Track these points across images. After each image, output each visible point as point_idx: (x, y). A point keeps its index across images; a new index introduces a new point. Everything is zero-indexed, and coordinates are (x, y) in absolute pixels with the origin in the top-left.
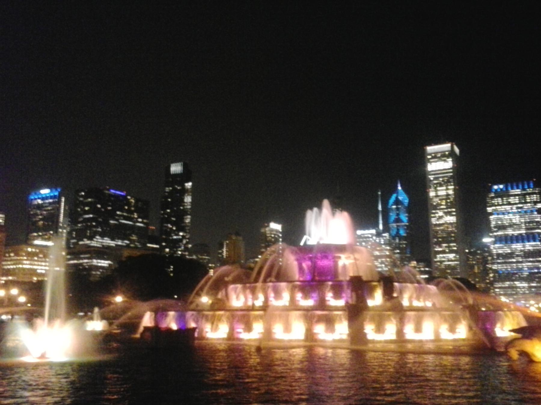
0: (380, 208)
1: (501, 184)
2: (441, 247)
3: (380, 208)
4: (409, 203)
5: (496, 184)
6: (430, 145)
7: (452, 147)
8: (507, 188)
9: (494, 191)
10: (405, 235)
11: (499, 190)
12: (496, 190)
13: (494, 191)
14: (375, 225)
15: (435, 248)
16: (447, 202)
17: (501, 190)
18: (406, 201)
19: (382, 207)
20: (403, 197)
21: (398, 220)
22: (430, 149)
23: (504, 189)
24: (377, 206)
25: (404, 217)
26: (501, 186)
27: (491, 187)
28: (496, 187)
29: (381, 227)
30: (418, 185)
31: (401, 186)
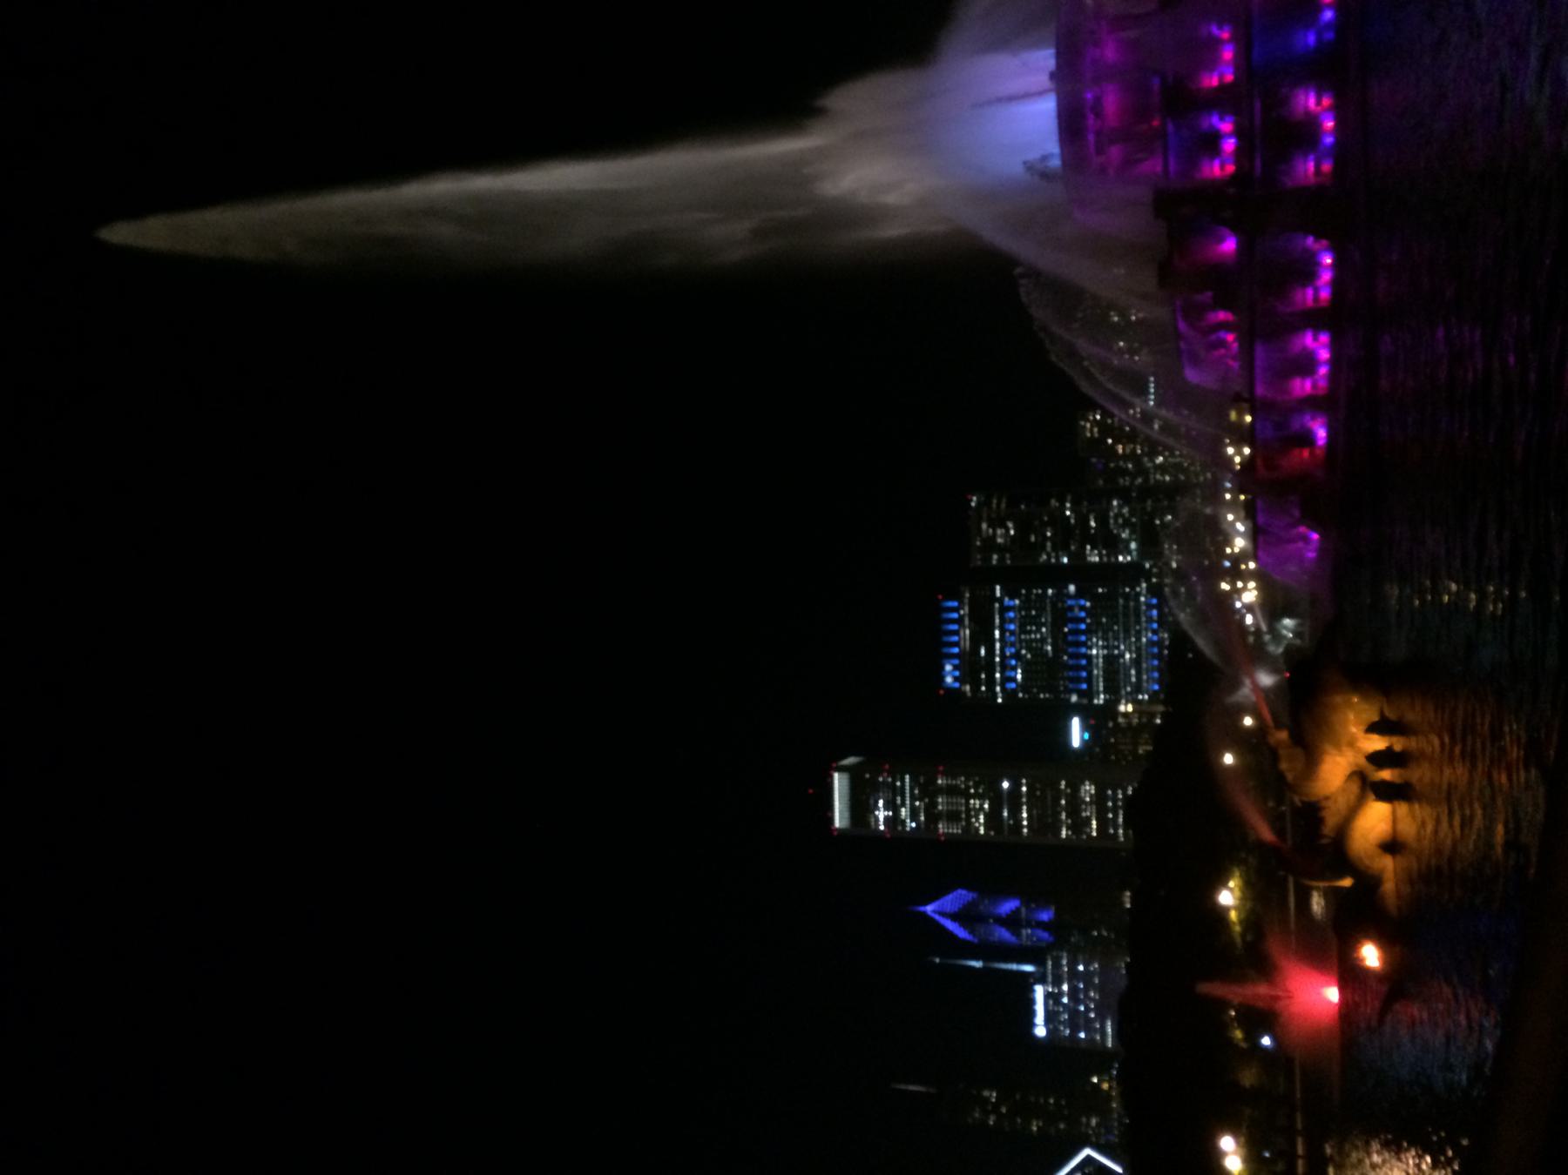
0: (978, 964)
1: (942, 668)
2: (1088, 821)
4: (969, 888)
5: (942, 678)
6: (831, 820)
7: (841, 769)
9: (957, 685)
10: (1053, 908)
11: (957, 673)
12: (956, 679)
13: (957, 685)
14: (1024, 985)
15: (1089, 836)
17: (956, 668)
18: (962, 892)
19: (976, 959)
20: (955, 899)
21: (1013, 922)
22: (839, 819)
23: (956, 662)
24: (973, 968)
25: (1008, 906)
26: (948, 668)
27: (949, 690)
28: (949, 680)
29: (1029, 968)
31: (926, 904)
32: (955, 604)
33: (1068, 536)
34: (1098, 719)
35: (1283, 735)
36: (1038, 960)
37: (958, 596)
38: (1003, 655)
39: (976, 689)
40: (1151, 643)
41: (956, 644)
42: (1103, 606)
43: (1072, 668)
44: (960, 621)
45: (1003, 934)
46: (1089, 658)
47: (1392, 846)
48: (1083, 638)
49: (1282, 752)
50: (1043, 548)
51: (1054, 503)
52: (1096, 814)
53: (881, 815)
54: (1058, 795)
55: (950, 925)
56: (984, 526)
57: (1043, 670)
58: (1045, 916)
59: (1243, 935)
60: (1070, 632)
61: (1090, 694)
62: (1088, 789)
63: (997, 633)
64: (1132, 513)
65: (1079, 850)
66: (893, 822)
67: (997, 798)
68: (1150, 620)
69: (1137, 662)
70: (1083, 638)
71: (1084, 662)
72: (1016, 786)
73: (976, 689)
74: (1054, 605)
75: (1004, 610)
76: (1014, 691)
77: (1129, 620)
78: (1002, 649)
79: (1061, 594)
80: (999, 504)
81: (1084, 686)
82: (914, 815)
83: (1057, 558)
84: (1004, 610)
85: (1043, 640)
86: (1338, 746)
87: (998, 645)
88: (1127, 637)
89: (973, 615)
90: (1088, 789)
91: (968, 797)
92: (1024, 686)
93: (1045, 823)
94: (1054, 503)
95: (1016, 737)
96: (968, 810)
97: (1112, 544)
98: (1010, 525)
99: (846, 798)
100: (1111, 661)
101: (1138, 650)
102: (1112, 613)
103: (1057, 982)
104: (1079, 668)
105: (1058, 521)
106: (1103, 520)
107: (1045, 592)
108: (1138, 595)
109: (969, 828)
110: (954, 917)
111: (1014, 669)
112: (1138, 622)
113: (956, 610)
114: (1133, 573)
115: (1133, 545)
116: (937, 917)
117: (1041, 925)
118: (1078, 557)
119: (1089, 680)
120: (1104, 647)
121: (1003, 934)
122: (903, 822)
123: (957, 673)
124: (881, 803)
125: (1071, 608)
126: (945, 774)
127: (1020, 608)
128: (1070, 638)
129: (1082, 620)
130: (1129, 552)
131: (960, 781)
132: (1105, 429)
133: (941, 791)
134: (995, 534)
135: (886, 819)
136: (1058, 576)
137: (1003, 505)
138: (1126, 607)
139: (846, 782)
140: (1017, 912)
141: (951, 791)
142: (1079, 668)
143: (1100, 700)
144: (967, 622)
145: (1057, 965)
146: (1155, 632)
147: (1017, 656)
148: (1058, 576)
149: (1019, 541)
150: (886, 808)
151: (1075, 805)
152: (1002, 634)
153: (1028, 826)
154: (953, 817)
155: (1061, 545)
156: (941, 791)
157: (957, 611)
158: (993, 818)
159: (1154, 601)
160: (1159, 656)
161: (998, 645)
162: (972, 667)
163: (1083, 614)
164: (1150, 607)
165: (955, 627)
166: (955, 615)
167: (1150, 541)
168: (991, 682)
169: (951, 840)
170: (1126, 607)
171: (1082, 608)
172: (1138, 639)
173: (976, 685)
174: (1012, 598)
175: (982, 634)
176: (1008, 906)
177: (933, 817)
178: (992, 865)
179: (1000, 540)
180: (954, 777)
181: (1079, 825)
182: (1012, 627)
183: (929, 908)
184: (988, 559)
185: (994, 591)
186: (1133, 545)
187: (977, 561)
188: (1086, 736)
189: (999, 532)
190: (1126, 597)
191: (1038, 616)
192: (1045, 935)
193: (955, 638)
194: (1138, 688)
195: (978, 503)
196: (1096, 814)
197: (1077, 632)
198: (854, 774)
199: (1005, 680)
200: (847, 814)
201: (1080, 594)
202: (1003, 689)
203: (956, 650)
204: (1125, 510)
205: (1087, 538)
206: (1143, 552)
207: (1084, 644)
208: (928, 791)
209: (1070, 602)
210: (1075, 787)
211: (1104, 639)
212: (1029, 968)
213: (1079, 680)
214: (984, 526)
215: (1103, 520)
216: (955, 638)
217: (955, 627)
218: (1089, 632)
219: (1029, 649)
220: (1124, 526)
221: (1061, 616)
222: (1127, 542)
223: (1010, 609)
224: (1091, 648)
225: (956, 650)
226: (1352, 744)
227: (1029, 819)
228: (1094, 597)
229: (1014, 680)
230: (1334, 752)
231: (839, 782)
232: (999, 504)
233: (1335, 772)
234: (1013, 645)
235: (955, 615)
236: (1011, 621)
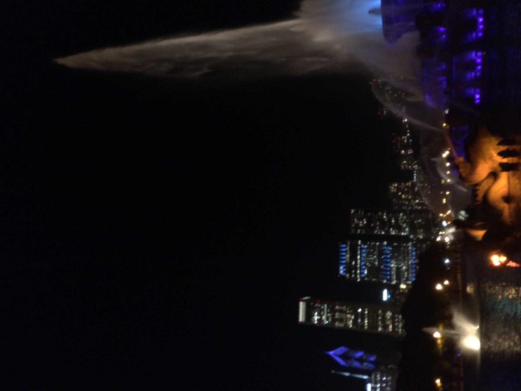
0: (347, 374)
1: (339, 267)
3: (347, 374)
4: (346, 346)
5: (338, 270)
6: (298, 318)
7: (303, 301)
8: (343, 264)
12: (344, 272)
13: (344, 274)
16: (349, 313)
17: (344, 268)
20: (341, 350)
21: (360, 360)
22: (301, 318)
23: (344, 266)
25: (359, 354)
26: (341, 268)
28: (341, 272)
29: (365, 377)
30: (331, 335)
31: (330, 350)
32: (344, 246)
33: (384, 225)
34: (393, 290)
35: (461, 159)
36: (369, 375)
37: (347, 244)
38: (360, 264)
39: (350, 275)
40: (412, 264)
41: (344, 260)
42: (396, 250)
43: (384, 270)
44: (346, 252)
45: (357, 364)
46: (391, 268)
47: (507, 199)
48: (389, 260)
49: (460, 165)
50: (376, 229)
51: (380, 213)
52: (392, 324)
53: (316, 318)
54: (378, 316)
55: (339, 360)
56: (356, 220)
57: (374, 271)
58: (373, 359)
59: (443, 348)
60: (384, 258)
61: (390, 280)
62: (389, 314)
63: (359, 257)
64: (407, 218)
65: (385, 336)
66: (320, 320)
67: (357, 315)
68: (412, 256)
69: (407, 270)
70: (389, 260)
71: (388, 269)
72: (363, 311)
73: (350, 275)
74: (379, 248)
75: (361, 249)
76: (364, 278)
77: (405, 255)
78: (361, 262)
79: (381, 245)
80: (361, 213)
81: (389, 277)
82: (327, 319)
83: (381, 232)
84: (361, 249)
85: (374, 260)
86: (485, 160)
87: (359, 261)
88: (404, 261)
89: (350, 250)
90: (389, 314)
91: (347, 314)
92: (367, 276)
93: (373, 325)
94: (380, 213)
95: (364, 294)
96: (346, 319)
97: (400, 229)
98: (365, 220)
99: (304, 311)
100: (398, 269)
101: (408, 266)
102: (399, 252)
103: (376, 383)
104: (387, 271)
105: (381, 219)
106: (397, 220)
107: (375, 244)
108: (408, 247)
109: (346, 325)
110: (340, 356)
111: (364, 269)
112: (408, 256)
113: (345, 248)
114: (406, 239)
115: (407, 229)
116: (334, 356)
117: (370, 362)
118: (388, 232)
119: (390, 275)
120: (396, 264)
121: (357, 364)
122: (323, 321)
123: (344, 270)
124: (316, 314)
125: (385, 250)
126: (339, 305)
127: (367, 249)
128: (384, 260)
129: (389, 254)
130: (405, 231)
131: (344, 308)
132: (398, 189)
133: (336, 311)
134: (359, 224)
135: (318, 320)
136: (381, 238)
137: (363, 213)
138: (404, 250)
139: (304, 306)
140: (363, 355)
141: (341, 311)
142: (387, 271)
143: (394, 282)
144: (348, 252)
145: (376, 377)
146: (414, 260)
147: (365, 265)
148: (381, 238)
149: (368, 225)
150: (318, 315)
151: (384, 319)
152: (361, 257)
153: (368, 325)
154: (341, 320)
155: (382, 228)
156: (336, 311)
157: (345, 249)
158: (355, 322)
159: (414, 249)
160: (415, 268)
161: (359, 261)
162: (350, 268)
163: (389, 252)
164: (413, 251)
165: (344, 254)
166: (344, 250)
167: (413, 229)
168: (356, 274)
169: (340, 329)
170: (404, 250)
171: (389, 250)
172: (408, 262)
173: (351, 274)
174: (365, 245)
175: (353, 257)
176: (359, 354)
177: (334, 320)
178: (354, 339)
179: (361, 225)
180: (342, 307)
181: (385, 327)
182: (364, 255)
183: (331, 353)
184: (356, 231)
185: (358, 242)
186: (407, 229)
187: (353, 231)
188: (389, 296)
189: (361, 222)
190: (404, 247)
191: (373, 252)
192: (372, 366)
193: (344, 258)
194: (407, 279)
195: (354, 212)
196: (392, 324)
197: (387, 258)
198: (307, 303)
199: (361, 273)
200: (304, 317)
201: (388, 245)
202: (360, 277)
203: (344, 262)
204: (405, 217)
205: (391, 226)
206: (411, 232)
207: (389, 262)
208: (332, 311)
209: (385, 248)
210: (384, 312)
211: (396, 261)
212: (365, 377)
213: (387, 275)
214: (356, 220)
215: (397, 220)
216: (344, 258)
217: (344, 254)
218: (391, 258)
219: (370, 263)
220: (404, 223)
221: (381, 253)
222: (405, 228)
223: (363, 249)
224: (391, 264)
225: (344, 262)
226: (491, 158)
227: (368, 323)
228: (393, 247)
229: (363, 273)
230: (483, 162)
231: (302, 306)
232: (361, 212)
233: (483, 170)
234: (364, 261)
235: (344, 250)
236: (364, 253)
